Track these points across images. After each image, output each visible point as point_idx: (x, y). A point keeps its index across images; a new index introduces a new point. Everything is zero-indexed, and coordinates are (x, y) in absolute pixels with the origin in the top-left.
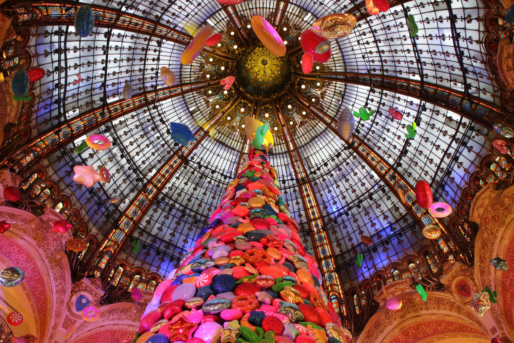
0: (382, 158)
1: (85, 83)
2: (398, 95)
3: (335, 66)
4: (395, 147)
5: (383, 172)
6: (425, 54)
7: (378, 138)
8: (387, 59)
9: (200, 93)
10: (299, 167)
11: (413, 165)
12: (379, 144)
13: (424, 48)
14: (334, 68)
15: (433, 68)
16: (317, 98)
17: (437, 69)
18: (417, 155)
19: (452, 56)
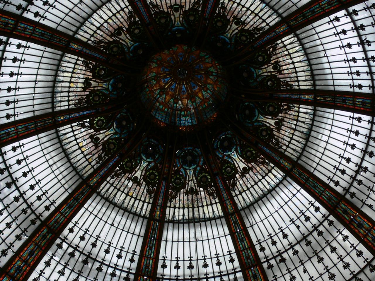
3: (288, 146)
8: (364, 181)
9: (87, 65)
14: (284, 147)
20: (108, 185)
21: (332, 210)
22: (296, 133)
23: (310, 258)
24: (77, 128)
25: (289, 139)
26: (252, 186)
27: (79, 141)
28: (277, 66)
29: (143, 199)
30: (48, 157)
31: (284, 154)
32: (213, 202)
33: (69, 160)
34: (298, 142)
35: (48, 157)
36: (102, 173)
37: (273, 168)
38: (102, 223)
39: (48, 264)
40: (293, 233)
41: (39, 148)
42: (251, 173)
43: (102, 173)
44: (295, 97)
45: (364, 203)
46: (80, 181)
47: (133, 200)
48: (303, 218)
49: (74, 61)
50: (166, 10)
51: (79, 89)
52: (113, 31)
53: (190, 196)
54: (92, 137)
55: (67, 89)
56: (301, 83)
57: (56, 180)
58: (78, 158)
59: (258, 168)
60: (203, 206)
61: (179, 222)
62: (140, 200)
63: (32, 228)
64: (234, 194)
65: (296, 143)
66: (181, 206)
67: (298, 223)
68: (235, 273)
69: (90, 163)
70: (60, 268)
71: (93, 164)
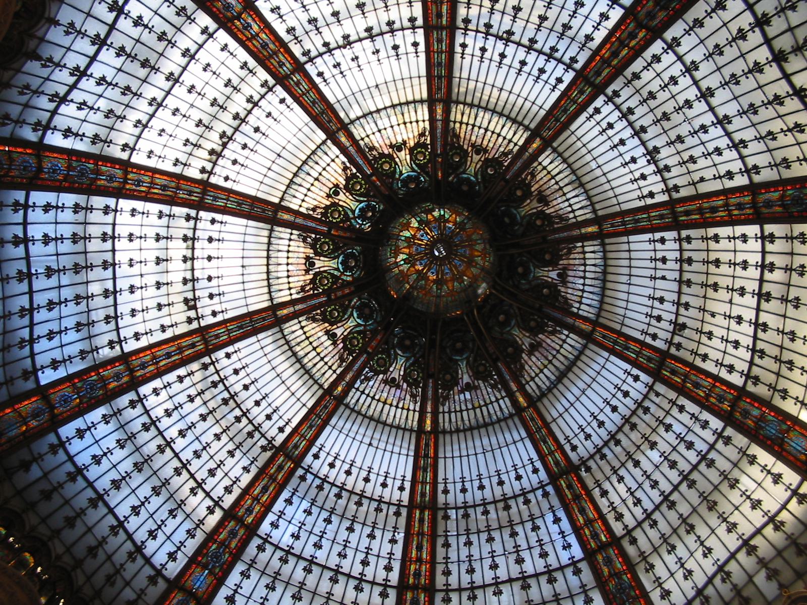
0: (716, 378)
1: (71, 308)
2: (712, 231)
3: (573, 211)
4: (736, 344)
5: (726, 406)
6: (738, 123)
7: (696, 337)
8: (670, 162)
9: (314, 320)
10: (545, 442)
11: (784, 371)
12: (703, 350)
13: (731, 109)
14: (571, 215)
15: (761, 147)
16: (552, 287)
17: (772, 144)
18: (787, 343)
19: (787, 101)
20: (447, 415)
21: (677, 226)
22: (566, 190)
23: (705, 297)
24: (363, 386)
25: (572, 204)
26: (584, 285)
27: (377, 397)
28: (479, 149)
29: (493, 399)
30: (359, 437)
31: (577, 222)
32: (564, 337)
33: (385, 424)
34: (577, 196)
35: (359, 437)
36: (429, 409)
37: (583, 247)
38: (472, 458)
39: (447, 545)
40: (668, 289)
41: (342, 436)
42: (570, 273)
43: (429, 409)
44: (525, 159)
45: (694, 184)
46: (414, 435)
47: (484, 409)
48: (659, 265)
49: (298, 326)
50: (328, 203)
51: (331, 348)
52: (303, 267)
53: (537, 354)
54: (385, 382)
55: (318, 358)
56: (515, 140)
57: (388, 454)
58: (392, 414)
59: (571, 262)
60: (558, 352)
61: (550, 390)
62: (492, 403)
63: (402, 521)
64: (575, 310)
65: (576, 200)
66: (537, 371)
67: (659, 274)
68: (651, 388)
69: (408, 410)
70: (463, 539)
71: (412, 407)
